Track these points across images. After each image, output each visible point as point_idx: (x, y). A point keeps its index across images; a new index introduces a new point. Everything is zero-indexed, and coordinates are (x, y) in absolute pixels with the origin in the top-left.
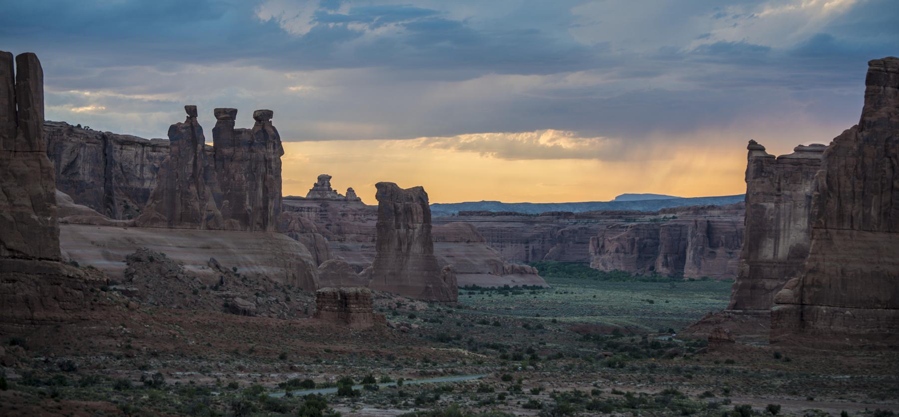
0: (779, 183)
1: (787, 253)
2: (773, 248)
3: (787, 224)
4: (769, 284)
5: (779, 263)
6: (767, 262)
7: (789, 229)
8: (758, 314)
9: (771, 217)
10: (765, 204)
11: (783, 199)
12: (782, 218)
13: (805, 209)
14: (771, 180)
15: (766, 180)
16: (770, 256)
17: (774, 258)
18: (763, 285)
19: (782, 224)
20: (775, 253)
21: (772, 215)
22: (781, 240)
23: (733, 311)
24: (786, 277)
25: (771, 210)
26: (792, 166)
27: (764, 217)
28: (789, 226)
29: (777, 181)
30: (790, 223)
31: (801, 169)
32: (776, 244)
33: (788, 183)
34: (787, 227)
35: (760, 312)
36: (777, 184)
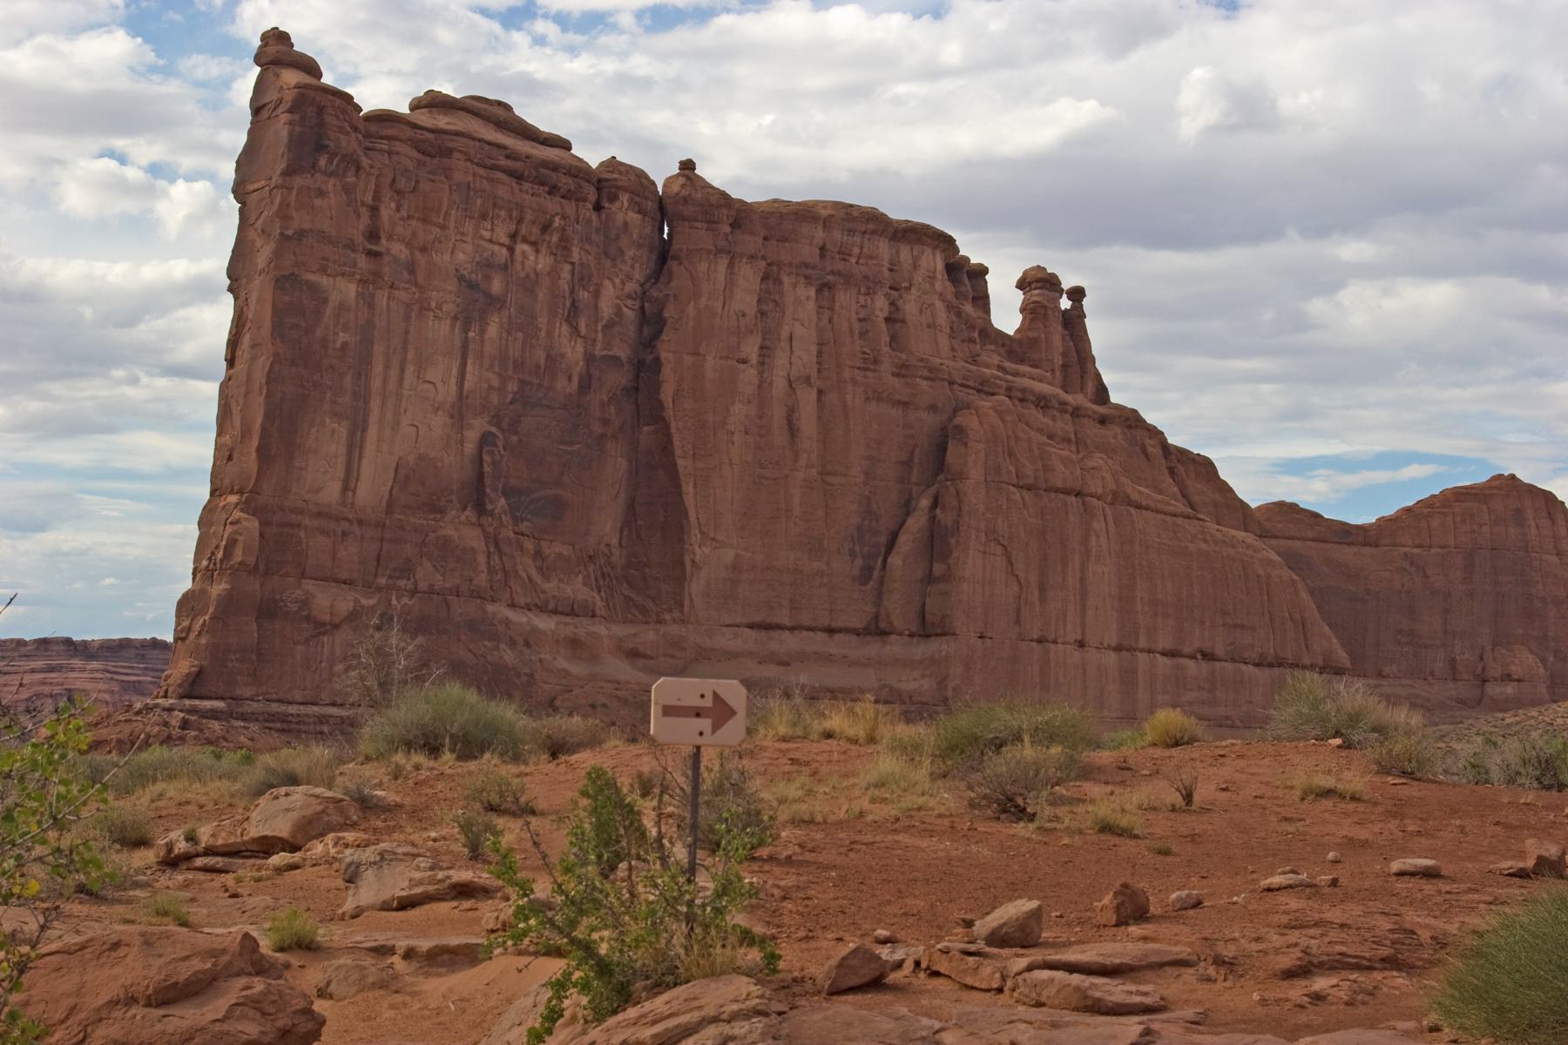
0: (374, 210)
1: (385, 490)
2: (342, 460)
3: (394, 373)
4: (328, 601)
5: (360, 522)
6: (319, 515)
7: (399, 396)
8: (284, 718)
9: (343, 337)
10: (325, 281)
11: (386, 270)
12: (379, 349)
13: (453, 327)
14: (348, 189)
15: (331, 185)
16: (331, 493)
17: (343, 504)
18: (305, 603)
19: (378, 368)
20: (348, 486)
21: (345, 328)
22: (372, 431)
23: (187, 702)
24: (383, 581)
25: (342, 307)
26: (414, 153)
27: (319, 333)
28: (401, 380)
29: (369, 199)
30: (402, 370)
31: (447, 173)
32: (355, 448)
33: (404, 213)
34: (392, 386)
35: (292, 709)
36: (364, 212)
